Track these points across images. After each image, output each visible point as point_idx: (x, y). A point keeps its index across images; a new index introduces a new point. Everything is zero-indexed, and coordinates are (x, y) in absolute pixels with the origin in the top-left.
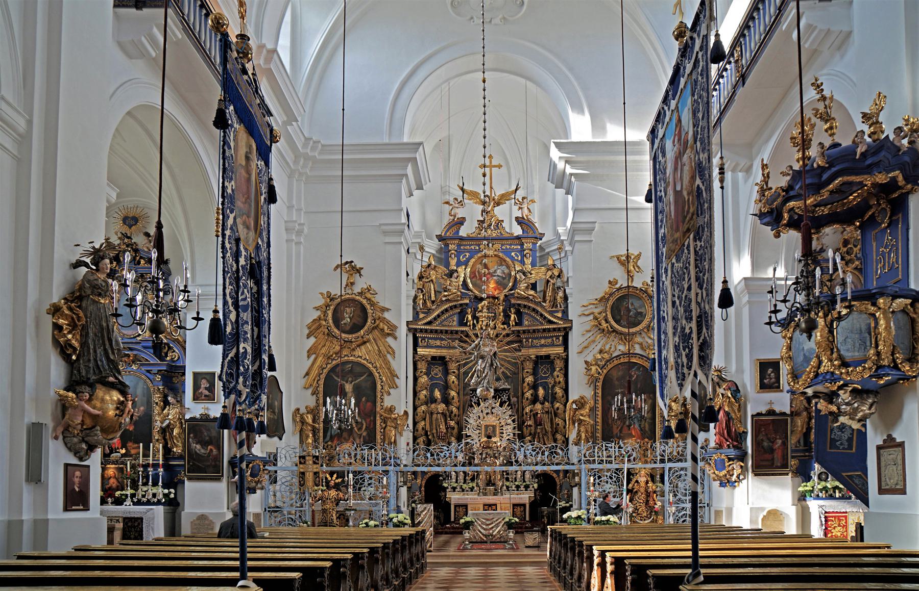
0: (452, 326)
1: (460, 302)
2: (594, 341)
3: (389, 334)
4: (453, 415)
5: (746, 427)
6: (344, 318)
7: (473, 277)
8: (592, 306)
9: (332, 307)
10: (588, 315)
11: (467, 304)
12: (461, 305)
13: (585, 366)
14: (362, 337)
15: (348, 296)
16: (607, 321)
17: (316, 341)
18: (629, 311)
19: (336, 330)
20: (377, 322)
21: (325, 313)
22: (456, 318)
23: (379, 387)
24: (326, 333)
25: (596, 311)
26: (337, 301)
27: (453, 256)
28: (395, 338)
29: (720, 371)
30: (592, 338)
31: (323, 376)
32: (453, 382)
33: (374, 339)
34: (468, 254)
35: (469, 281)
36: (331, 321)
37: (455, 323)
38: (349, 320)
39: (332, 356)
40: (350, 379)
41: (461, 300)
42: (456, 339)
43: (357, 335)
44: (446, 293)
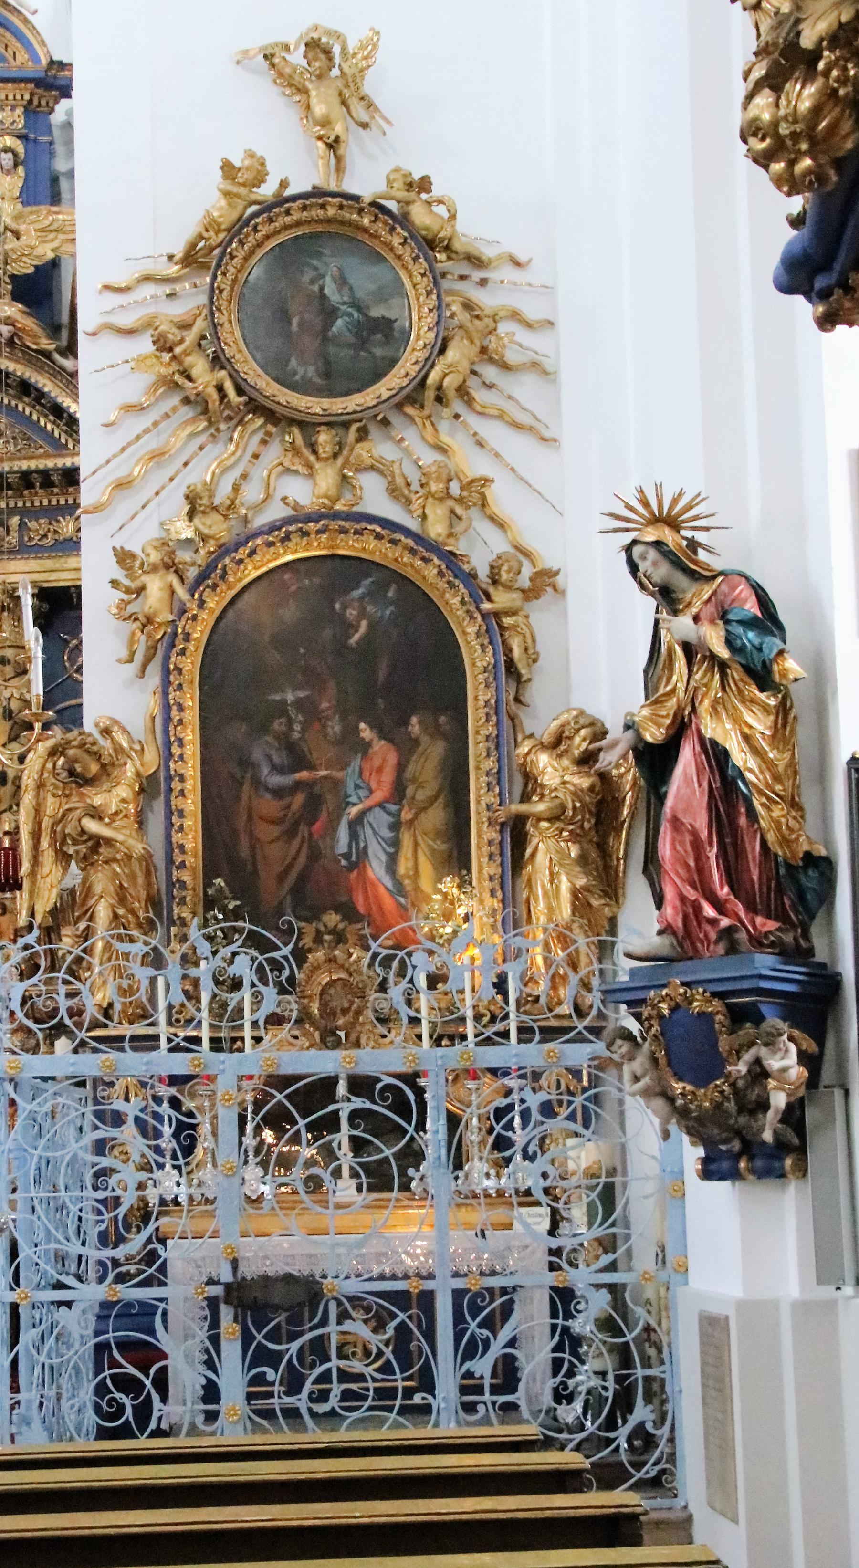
2: (157, 456)
5: (828, 842)
8: (148, 290)
10: (130, 332)
13: (119, 574)
16: (217, 361)
18: (329, 313)
25: (178, 310)
29: (673, 523)
30: (150, 443)
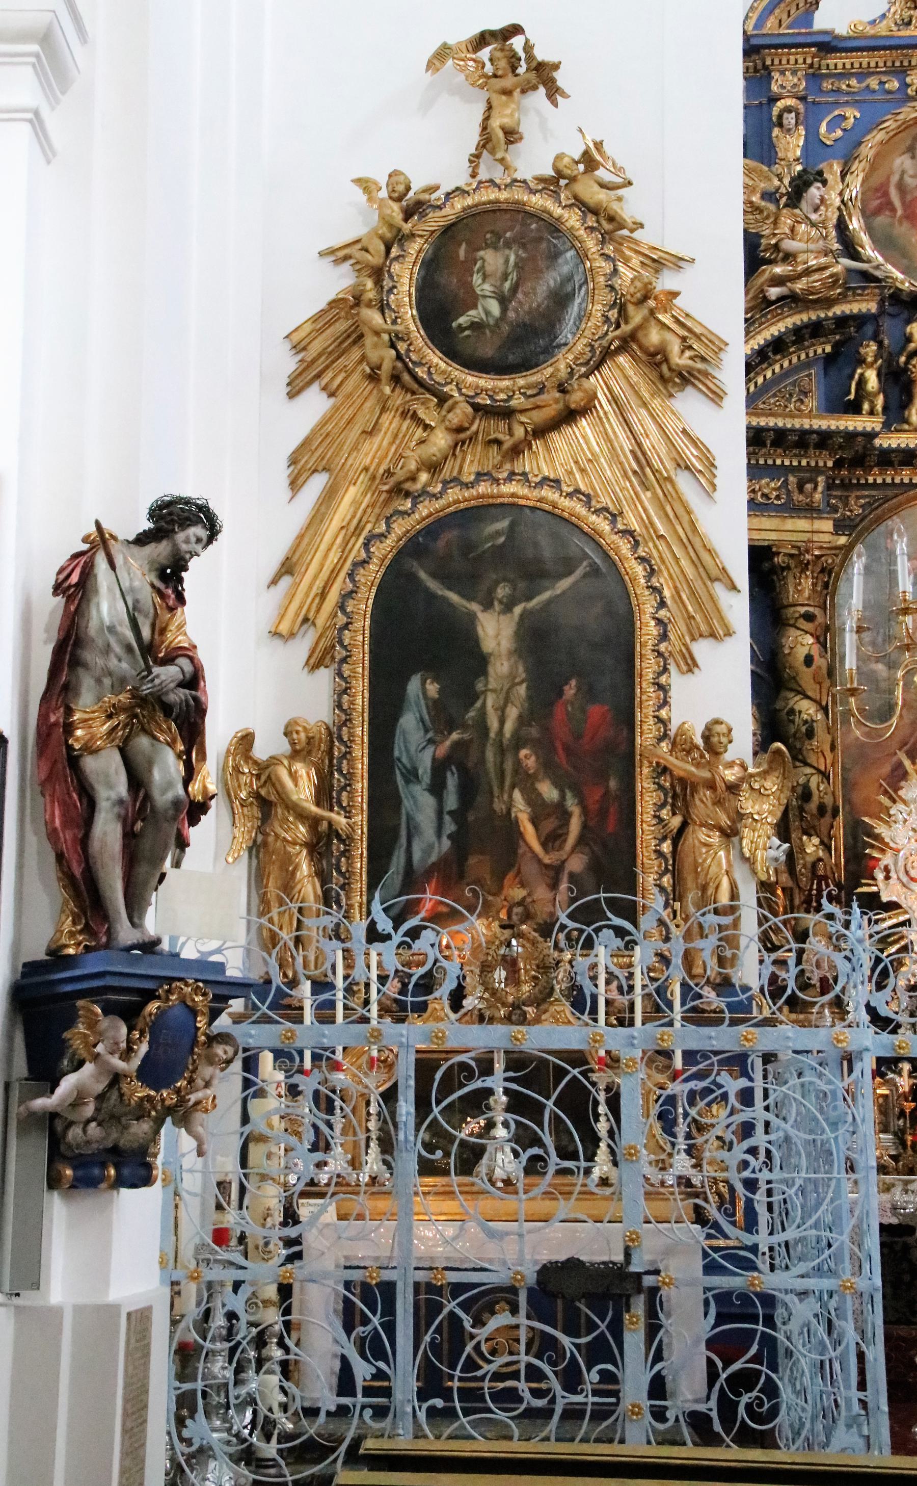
0: (800, 414)
1: (838, 310)
3: (686, 378)
4: (813, 806)
6: (472, 301)
7: (878, 211)
9: (414, 247)
11: (860, 320)
12: (842, 321)
14: (562, 389)
15: (492, 195)
17: (336, 409)
19: (435, 358)
20: (637, 316)
21: (378, 274)
22: (814, 379)
23: (648, 631)
24: (387, 366)
26: (435, 221)
27: (790, 119)
28: (717, 396)
31: (373, 573)
32: (809, 660)
33: (614, 400)
34: (852, 113)
35: (855, 224)
36: (409, 313)
37: (811, 403)
38: (495, 308)
39: (413, 478)
40: (502, 591)
41: (842, 298)
42: (817, 470)
43: (534, 377)
44: (778, 270)
